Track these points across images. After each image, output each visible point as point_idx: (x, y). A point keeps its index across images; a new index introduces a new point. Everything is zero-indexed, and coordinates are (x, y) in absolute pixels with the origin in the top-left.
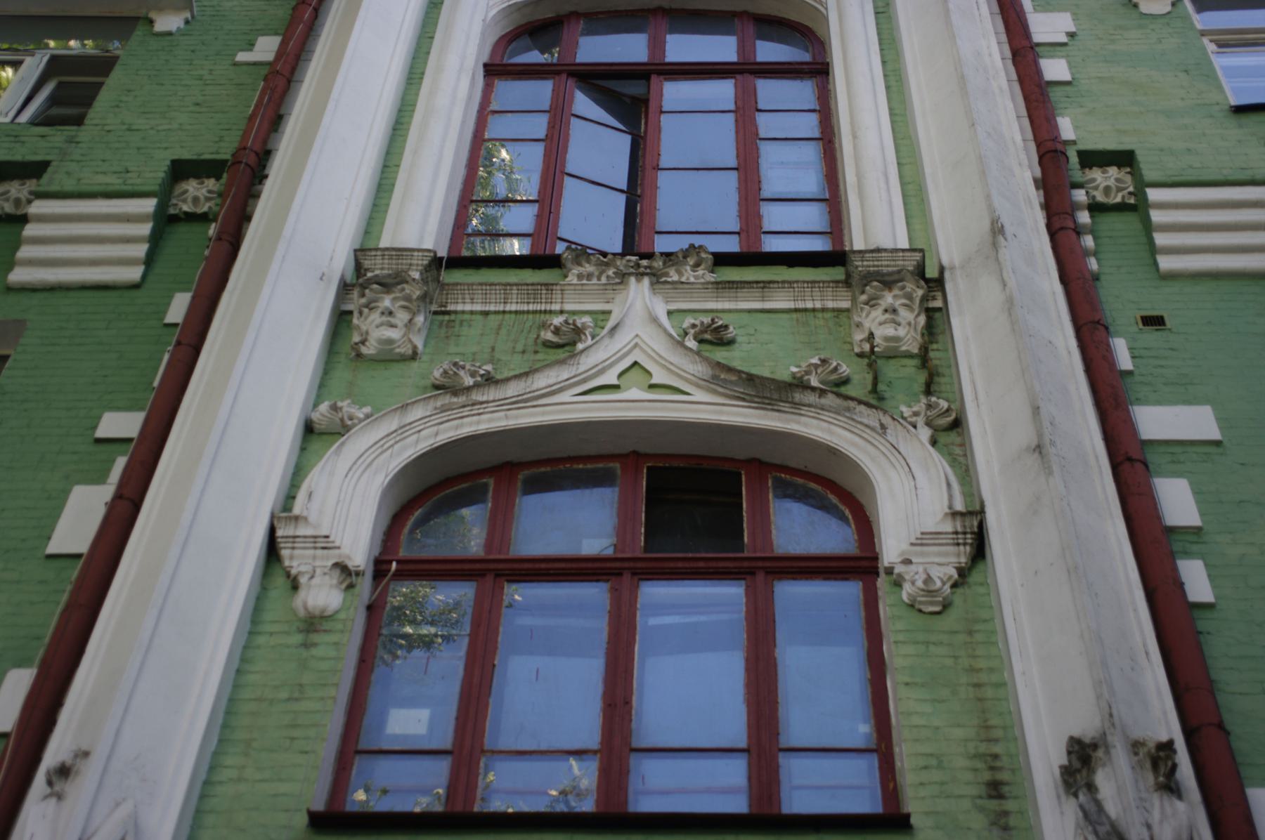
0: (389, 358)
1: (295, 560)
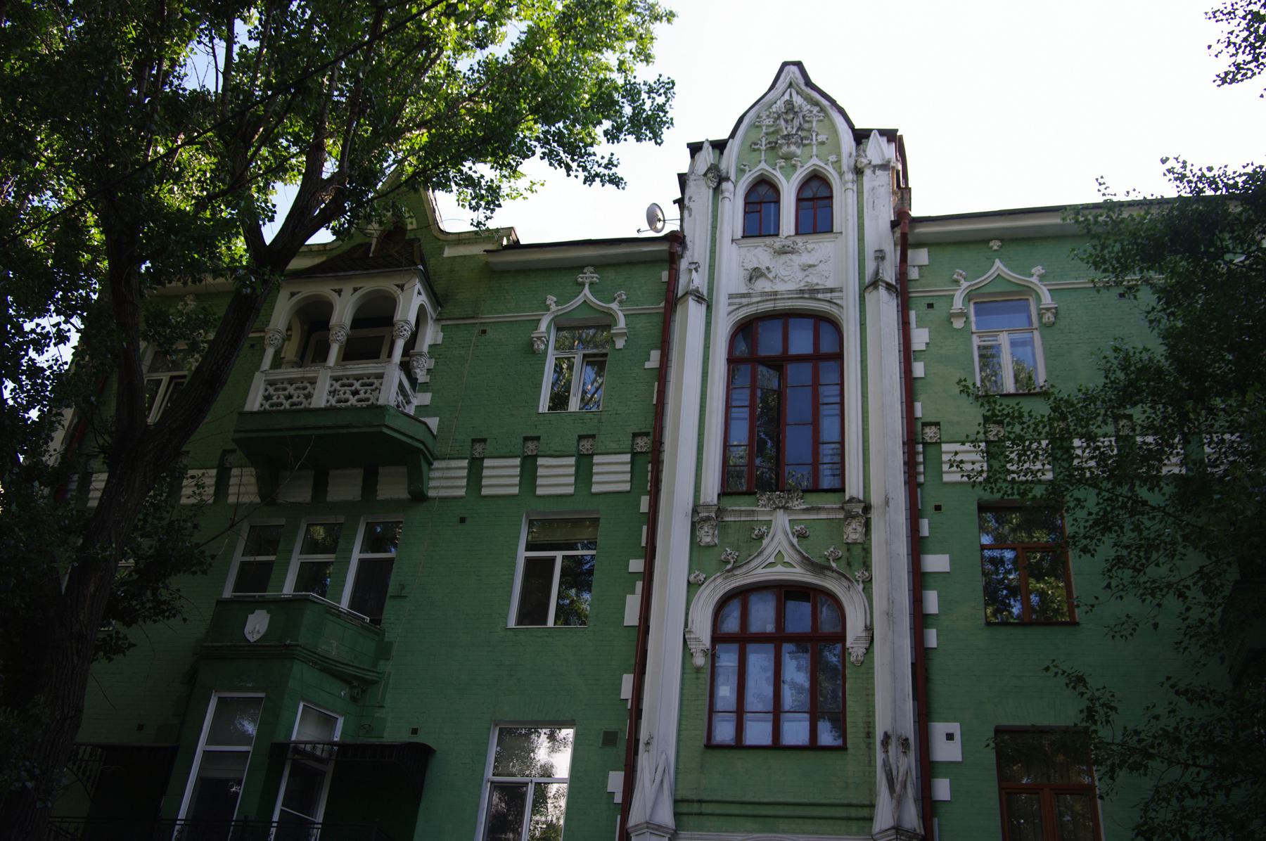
0: (708, 546)
1: (692, 646)
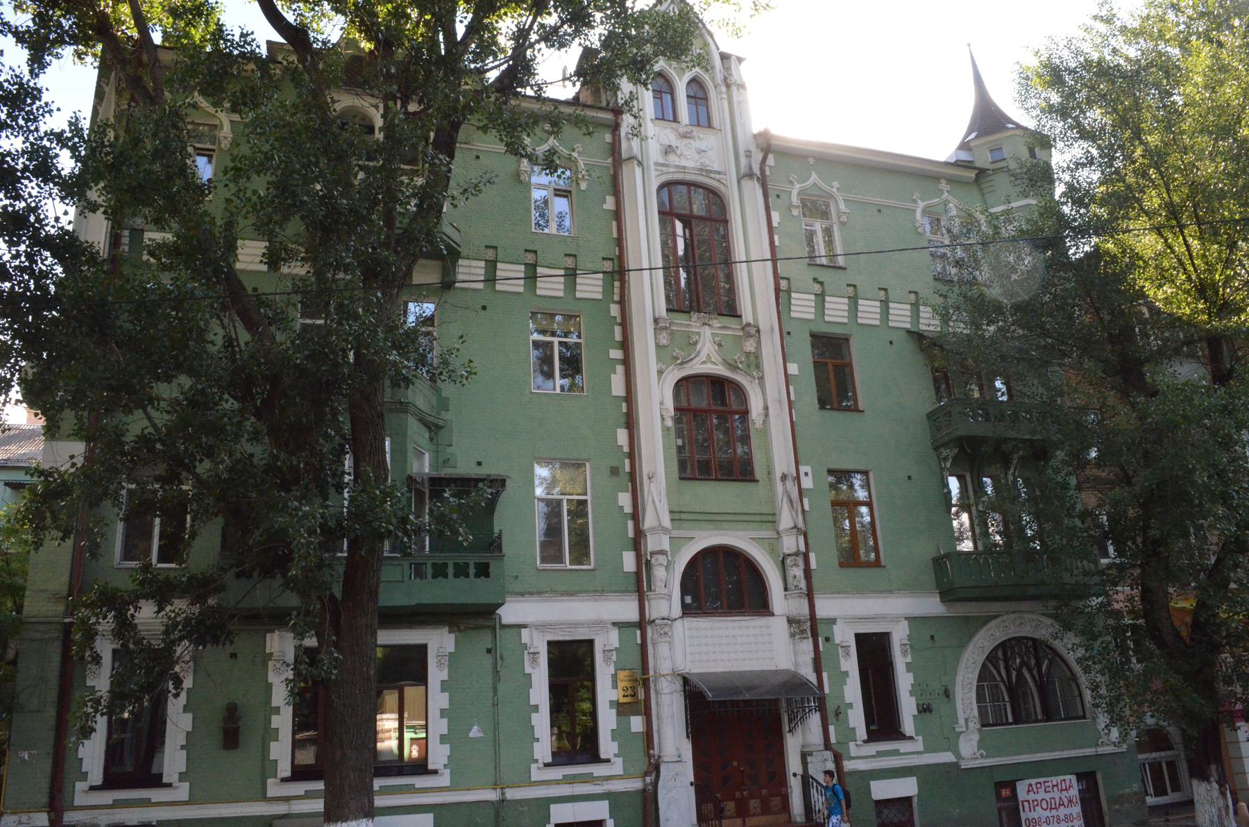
0: (664, 346)
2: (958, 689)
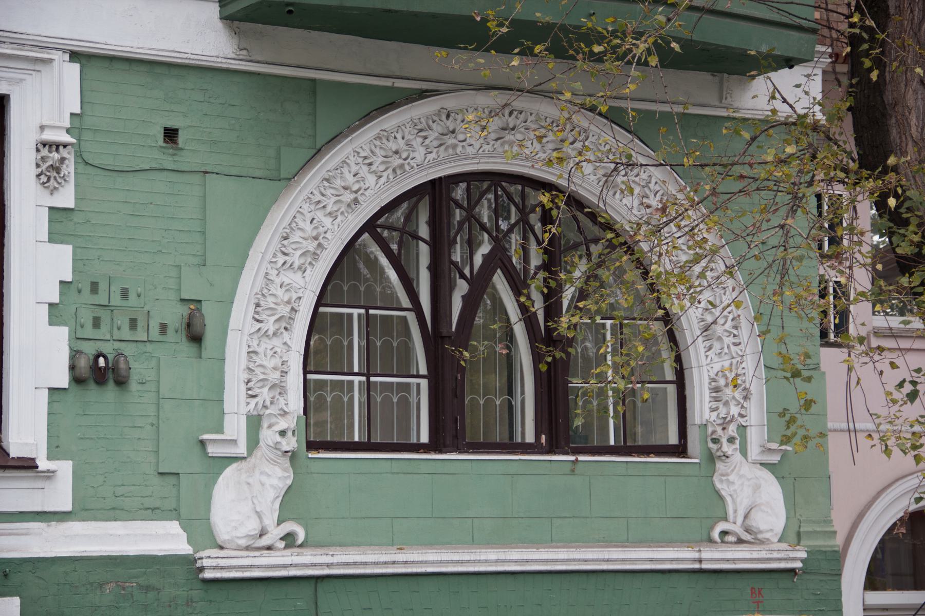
2: (240, 315)
